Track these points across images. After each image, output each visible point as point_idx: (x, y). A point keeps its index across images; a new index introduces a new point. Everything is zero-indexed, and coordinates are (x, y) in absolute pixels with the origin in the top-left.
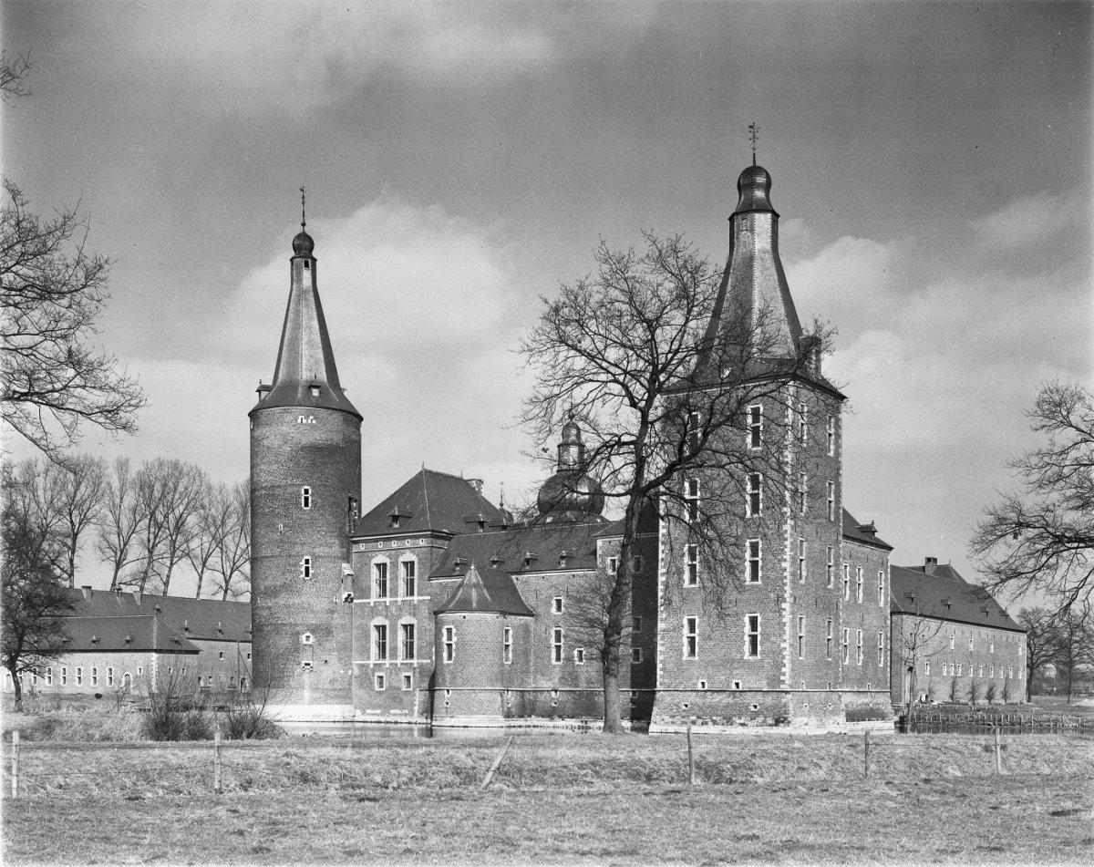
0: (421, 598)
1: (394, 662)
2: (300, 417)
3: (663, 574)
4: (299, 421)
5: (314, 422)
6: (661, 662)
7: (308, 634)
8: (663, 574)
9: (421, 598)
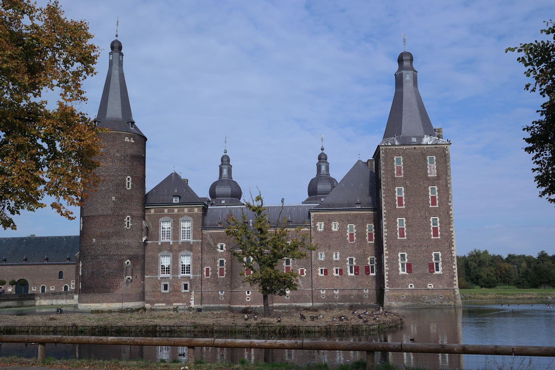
0: (195, 241)
1: (176, 276)
2: (126, 138)
3: (385, 232)
4: (126, 140)
5: (133, 141)
6: (387, 275)
7: (128, 261)
8: (385, 232)
9: (195, 241)
